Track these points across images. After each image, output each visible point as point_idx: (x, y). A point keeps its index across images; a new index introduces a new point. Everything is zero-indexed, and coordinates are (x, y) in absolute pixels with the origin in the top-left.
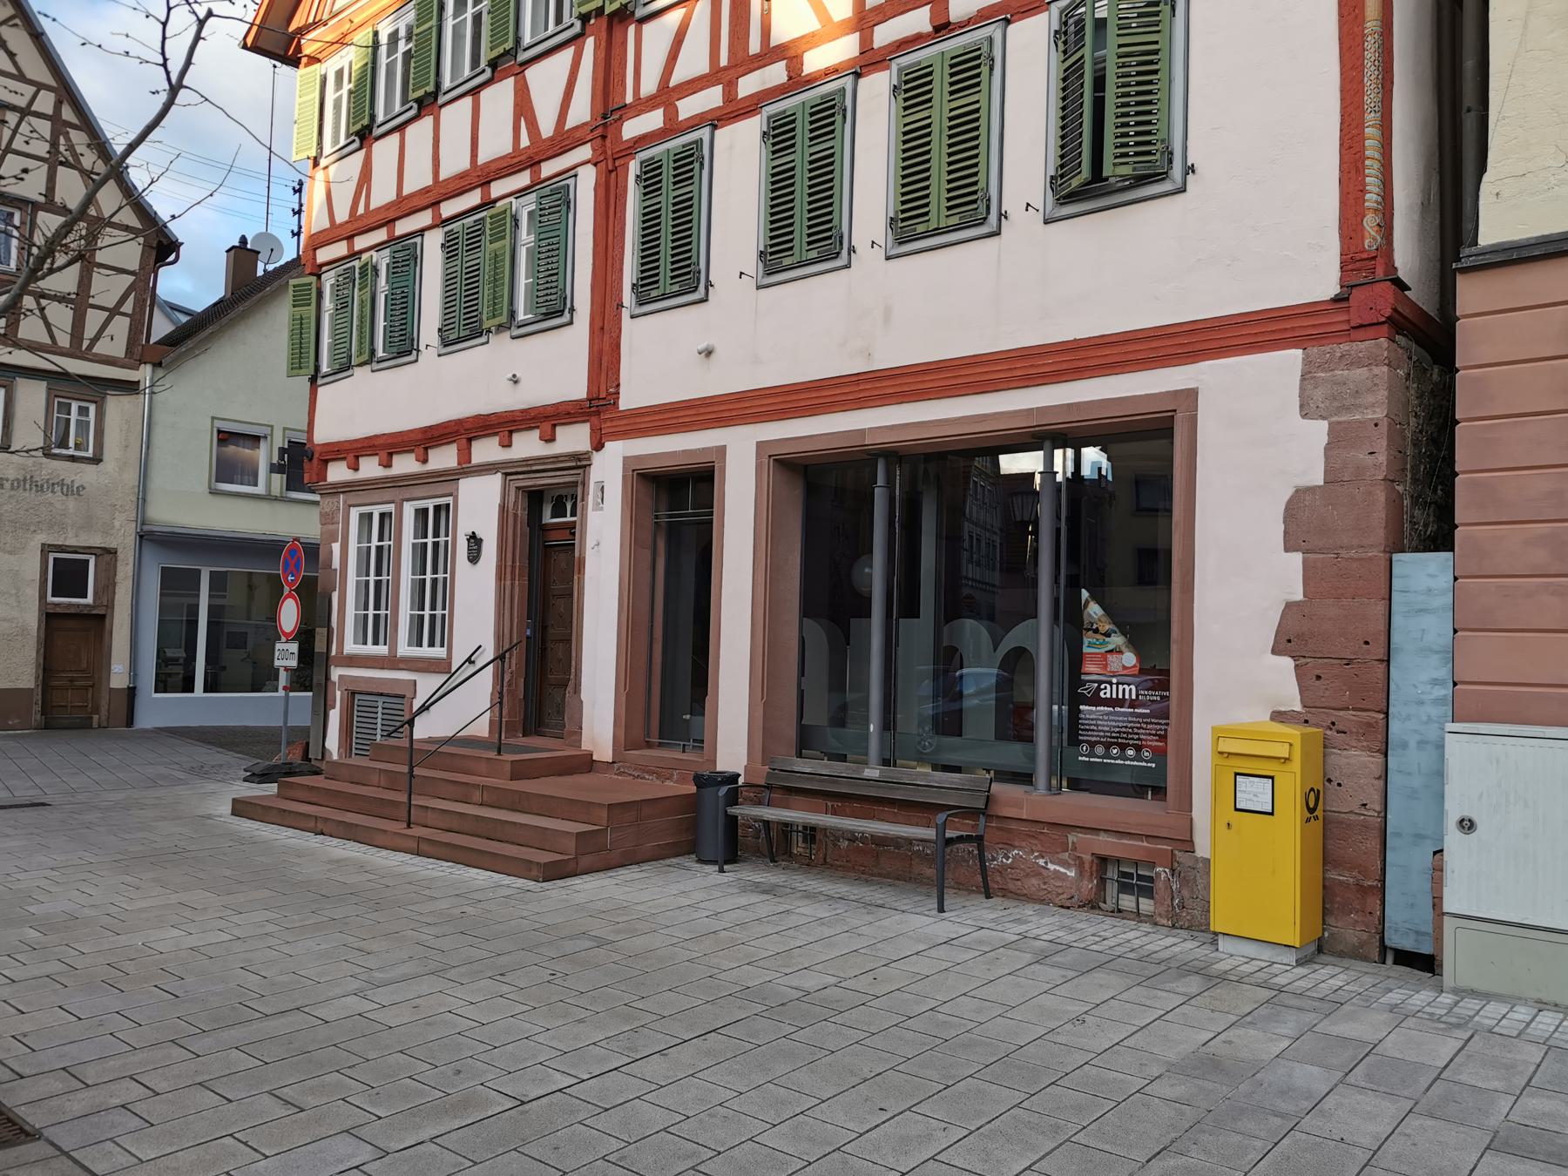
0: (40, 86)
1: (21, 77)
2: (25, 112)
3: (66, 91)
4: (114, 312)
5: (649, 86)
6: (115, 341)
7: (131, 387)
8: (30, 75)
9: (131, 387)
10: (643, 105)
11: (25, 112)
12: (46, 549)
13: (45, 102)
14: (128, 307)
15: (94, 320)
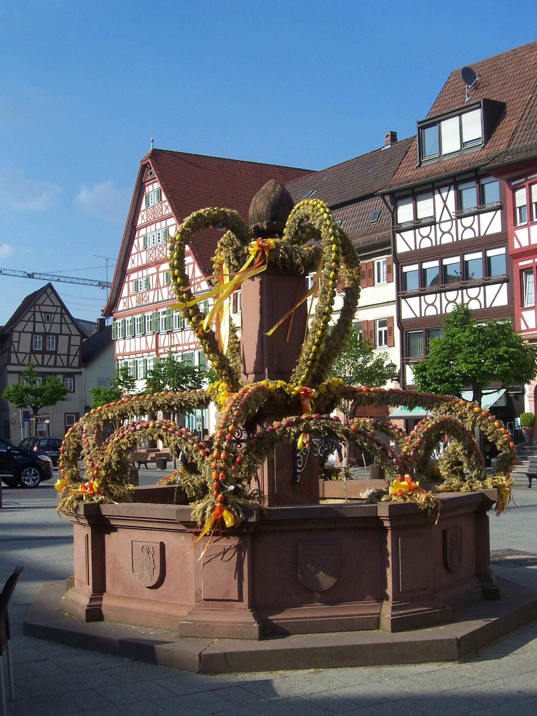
0: (58, 307)
1: (54, 306)
2: (55, 313)
3: (63, 307)
4: (75, 356)
5: (162, 346)
6: (76, 363)
7: (80, 373)
8: (56, 304)
9: (80, 373)
10: (162, 348)
11: (55, 313)
12: (65, 414)
13: (59, 310)
14: (78, 354)
15: (71, 358)
